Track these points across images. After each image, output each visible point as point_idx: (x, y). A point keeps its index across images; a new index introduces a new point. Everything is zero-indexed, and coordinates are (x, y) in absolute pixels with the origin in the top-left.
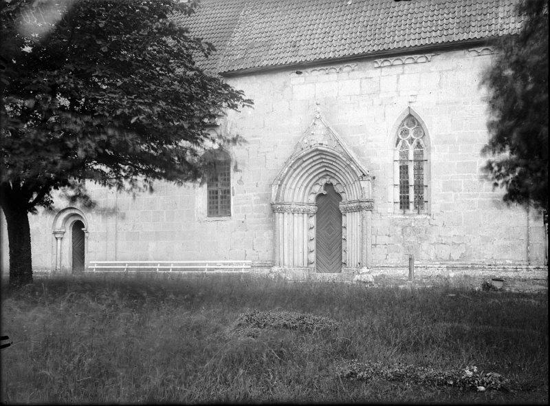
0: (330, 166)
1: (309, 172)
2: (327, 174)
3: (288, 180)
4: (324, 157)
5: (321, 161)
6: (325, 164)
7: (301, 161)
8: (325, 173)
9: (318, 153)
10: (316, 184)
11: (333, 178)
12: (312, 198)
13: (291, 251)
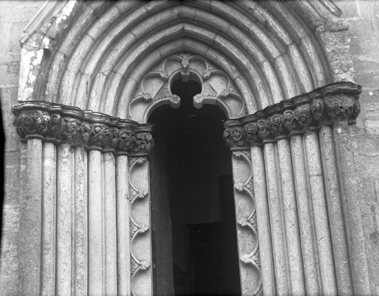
1: (137, 31)
2: (182, 45)
3: (75, 46)
8: (179, 44)
10: (148, 76)
11: (202, 59)
12: (140, 115)
13: (82, 272)
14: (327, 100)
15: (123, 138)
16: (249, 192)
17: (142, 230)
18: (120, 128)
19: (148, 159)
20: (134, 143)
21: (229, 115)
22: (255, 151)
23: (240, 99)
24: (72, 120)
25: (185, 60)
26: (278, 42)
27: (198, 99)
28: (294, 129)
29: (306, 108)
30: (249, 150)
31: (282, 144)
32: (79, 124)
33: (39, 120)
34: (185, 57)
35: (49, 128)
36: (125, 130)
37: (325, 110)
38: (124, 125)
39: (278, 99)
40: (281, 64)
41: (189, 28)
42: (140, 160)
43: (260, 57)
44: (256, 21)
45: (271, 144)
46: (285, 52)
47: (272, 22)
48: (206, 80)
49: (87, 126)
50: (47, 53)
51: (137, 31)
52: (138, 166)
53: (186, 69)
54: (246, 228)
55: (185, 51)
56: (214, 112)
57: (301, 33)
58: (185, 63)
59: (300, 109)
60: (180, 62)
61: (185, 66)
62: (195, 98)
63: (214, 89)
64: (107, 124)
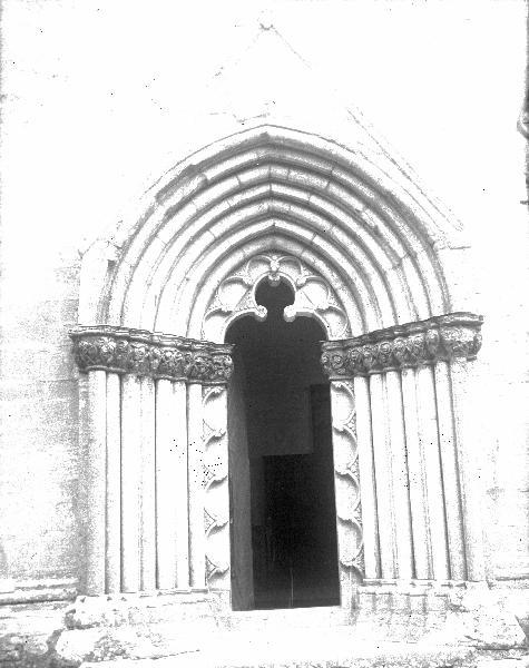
0: (296, 210)
1: (218, 230)
2: (273, 244)
4: (280, 172)
5: (263, 189)
6: (278, 205)
7: (195, 183)
8: (268, 242)
9: (262, 153)
10: (227, 281)
11: (296, 262)
12: (216, 332)
14: (444, 331)
15: (198, 364)
16: (350, 431)
17: (218, 478)
18: (194, 351)
19: (226, 386)
20: (210, 368)
21: (329, 333)
22: (359, 382)
23: (342, 314)
24: (139, 345)
25: (275, 261)
26: (392, 253)
27: (290, 312)
28: (406, 361)
29: (419, 338)
30: (352, 380)
31: (392, 376)
32: (147, 350)
33: (104, 349)
34: (275, 257)
35: (115, 356)
36: (199, 354)
37: (441, 342)
38: (197, 347)
39: (389, 323)
40: (392, 276)
41: (281, 224)
42: (217, 390)
43: (369, 268)
44: (363, 224)
45: (378, 376)
46: (398, 265)
47: (384, 229)
48: (299, 288)
49: (156, 351)
50: (111, 264)
51: (218, 230)
52: (214, 396)
53: (274, 274)
54: (347, 477)
55: (275, 251)
56: (310, 328)
57: (417, 246)
58: (275, 265)
59: (412, 338)
60: (269, 263)
61: (274, 269)
62: (286, 310)
63: (308, 300)
64: (181, 348)
